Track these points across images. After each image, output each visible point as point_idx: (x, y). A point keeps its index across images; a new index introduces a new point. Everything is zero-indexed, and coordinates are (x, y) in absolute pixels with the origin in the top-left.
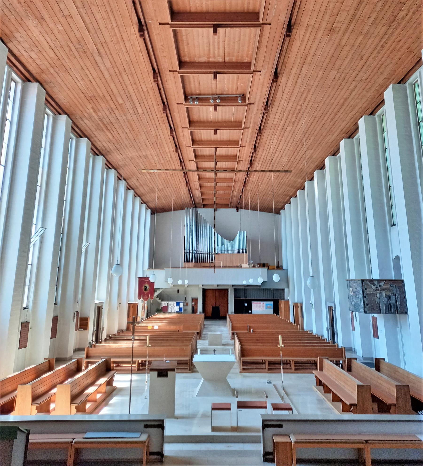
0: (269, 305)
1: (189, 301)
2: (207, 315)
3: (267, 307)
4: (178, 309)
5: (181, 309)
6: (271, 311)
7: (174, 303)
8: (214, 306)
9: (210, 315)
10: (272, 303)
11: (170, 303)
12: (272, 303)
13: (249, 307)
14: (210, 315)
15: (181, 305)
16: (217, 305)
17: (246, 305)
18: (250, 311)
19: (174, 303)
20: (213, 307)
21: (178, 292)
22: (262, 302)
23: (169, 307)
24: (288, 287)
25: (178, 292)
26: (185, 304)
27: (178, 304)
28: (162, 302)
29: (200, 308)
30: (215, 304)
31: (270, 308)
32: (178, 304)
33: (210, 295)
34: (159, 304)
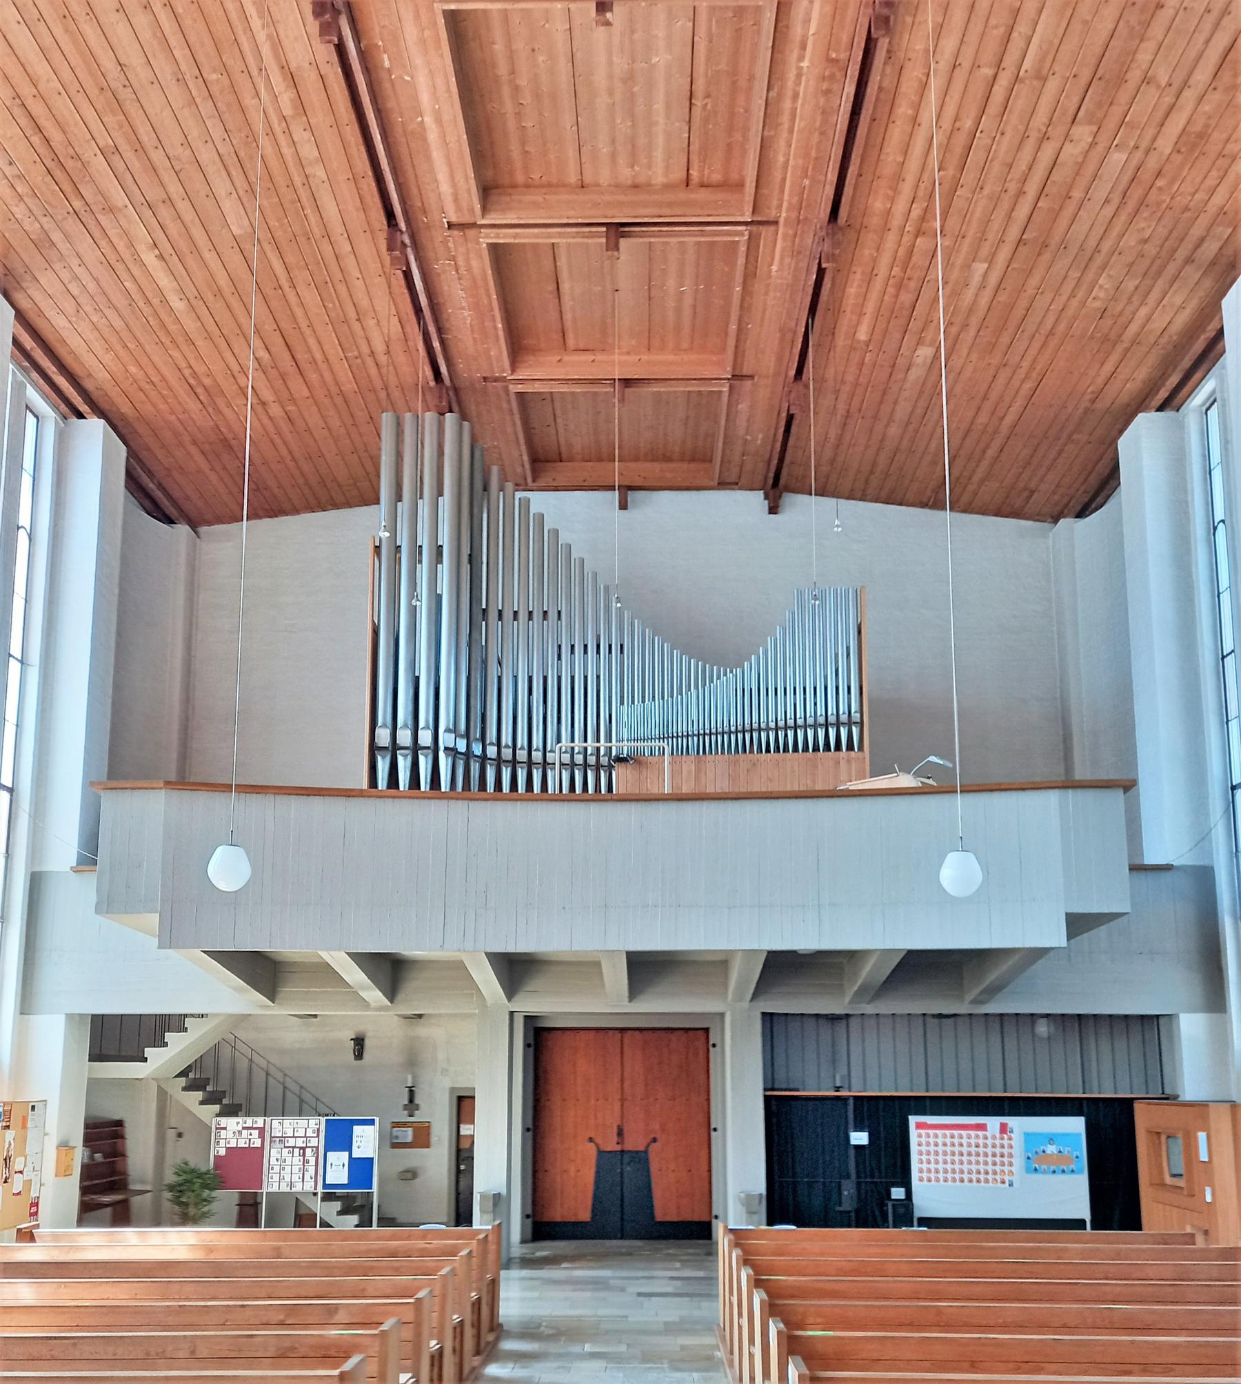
0: (1051, 1139)
1: (437, 1113)
2: (558, 1213)
3: (1037, 1162)
4: (338, 1173)
5: (360, 1168)
6: (1071, 1196)
7: (310, 1128)
8: (611, 1145)
9: (585, 1215)
10: (1076, 1125)
11: (277, 1126)
12: (1076, 1125)
13: (893, 1159)
14: (585, 1215)
15: (366, 1141)
16: (634, 1142)
17: (860, 1138)
18: (898, 1193)
19: (310, 1128)
20: (601, 1153)
21: (359, 1055)
22: (993, 1122)
23: (274, 1154)
24: (1214, 996)
25: (359, 1055)
26: (408, 1135)
27: (339, 1137)
28: (224, 1121)
29: (497, 1165)
30: (620, 1133)
31: (1059, 1166)
32: (339, 1137)
33: (575, 1070)
34: (204, 1132)
